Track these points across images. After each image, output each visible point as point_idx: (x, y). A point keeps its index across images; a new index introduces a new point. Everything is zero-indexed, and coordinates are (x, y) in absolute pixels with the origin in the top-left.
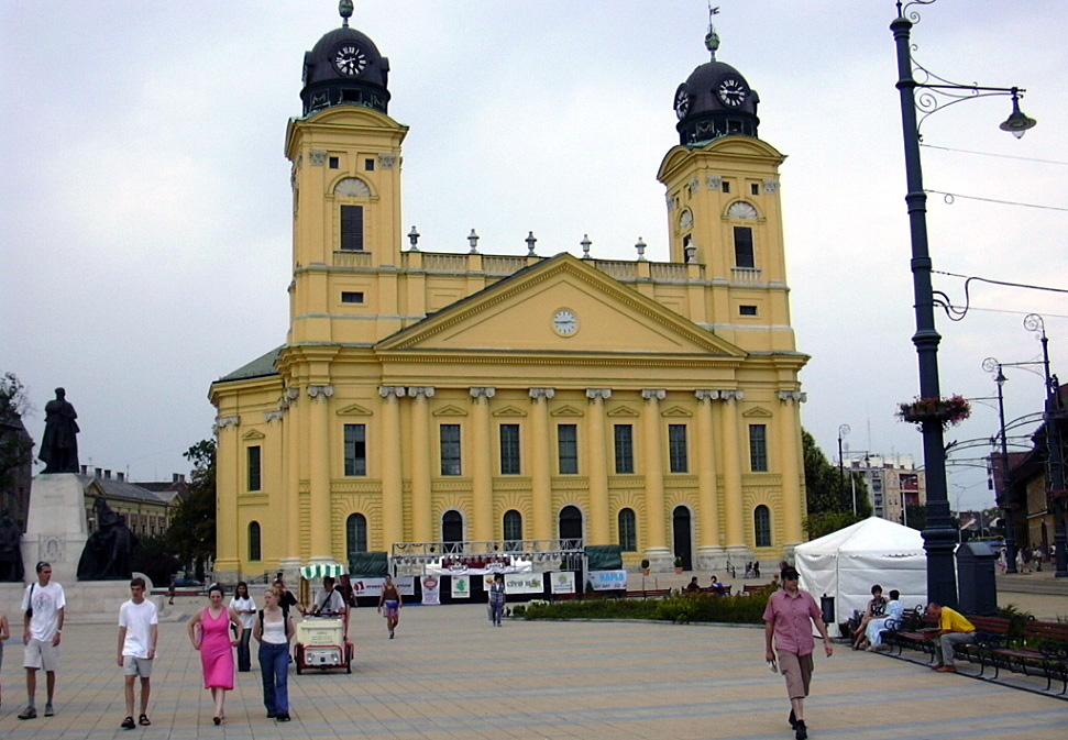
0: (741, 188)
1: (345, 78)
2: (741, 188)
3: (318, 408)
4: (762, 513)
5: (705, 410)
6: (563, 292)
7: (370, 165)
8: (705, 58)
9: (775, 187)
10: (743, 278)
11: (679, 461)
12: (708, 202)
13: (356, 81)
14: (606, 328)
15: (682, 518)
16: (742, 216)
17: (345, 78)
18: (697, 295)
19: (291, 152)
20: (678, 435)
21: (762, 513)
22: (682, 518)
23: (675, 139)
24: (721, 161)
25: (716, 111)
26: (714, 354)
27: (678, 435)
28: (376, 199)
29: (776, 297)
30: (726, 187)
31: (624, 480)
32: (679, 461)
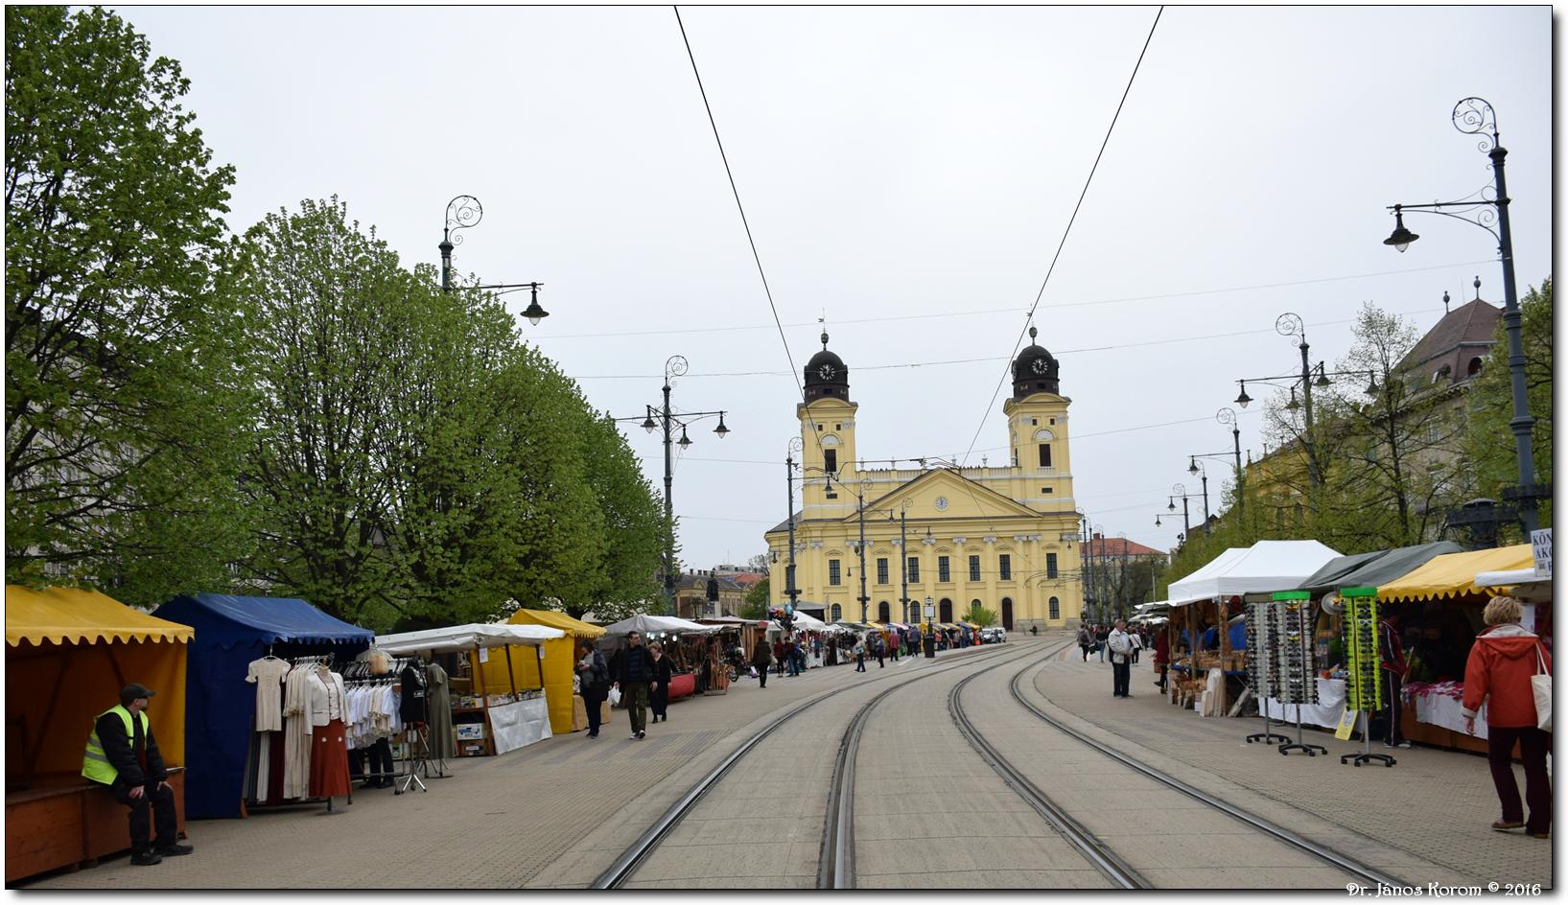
0: (1043, 422)
1: (826, 379)
2: (1043, 422)
3: (817, 553)
4: (1054, 601)
5: (1020, 548)
6: (942, 488)
7: (838, 427)
8: (1027, 342)
9: (1065, 419)
10: (1045, 472)
11: (1005, 572)
12: (1026, 430)
13: (829, 383)
14: (962, 504)
15: (1007, 604)
16: (1044, 438)
17: (826, 379)
18: (1016, 484)
19: (800, 416)
20: (1005, 561)
21: (1054, 601)
22: (1007, 604)
23: (1011, 395)
24: (1038, 405)
25: (1035, 374)
26: (1025, 515)
27: (1005, 561)
28: (842, 444)
29: (1064, 482)
30: (1035, 422)
31: (975, 585)
32: (1005, 572)
